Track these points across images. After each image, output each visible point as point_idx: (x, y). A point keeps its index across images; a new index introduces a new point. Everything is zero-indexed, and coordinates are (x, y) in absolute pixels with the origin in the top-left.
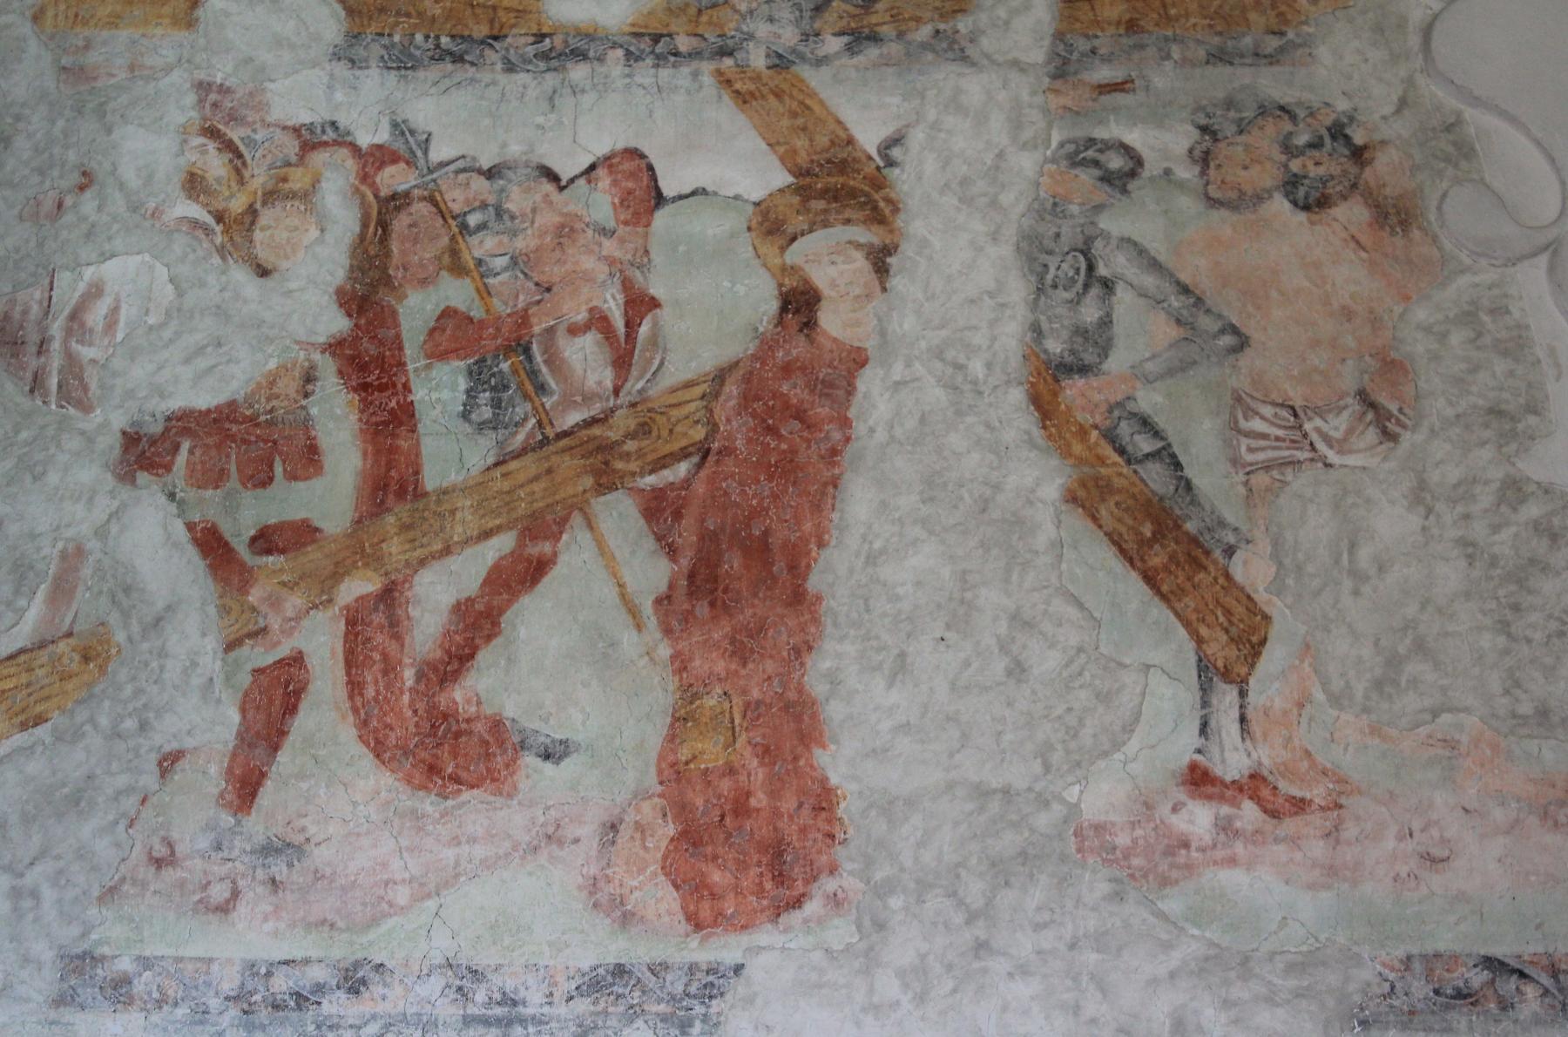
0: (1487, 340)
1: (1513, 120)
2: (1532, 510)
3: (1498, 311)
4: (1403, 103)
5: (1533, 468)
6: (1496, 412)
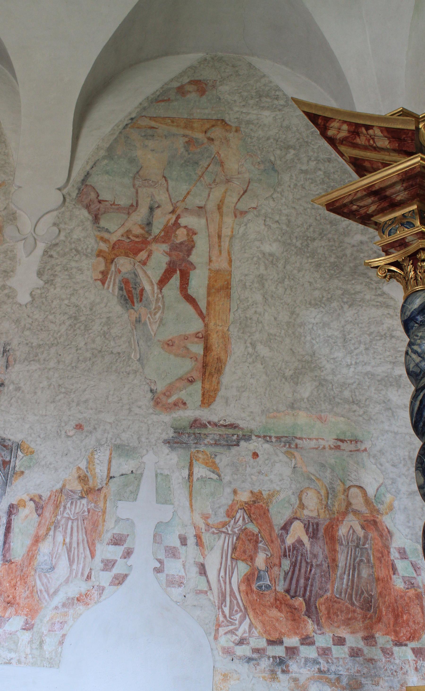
0: (8, 257)
1: (25, 213)
2: (6, 291)
3: (11, 251)
4: (5, 208)
5: (8, 283)
6: (5, 271)
